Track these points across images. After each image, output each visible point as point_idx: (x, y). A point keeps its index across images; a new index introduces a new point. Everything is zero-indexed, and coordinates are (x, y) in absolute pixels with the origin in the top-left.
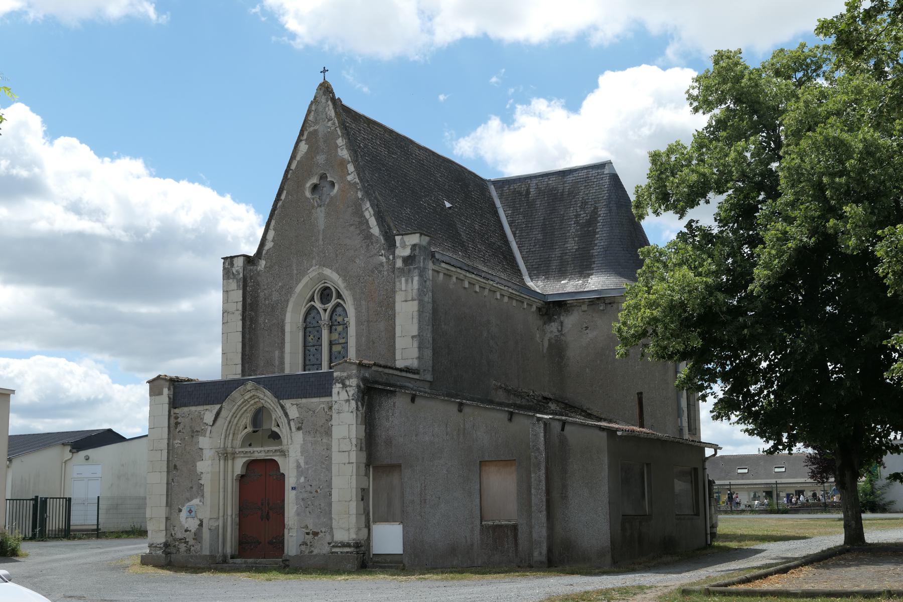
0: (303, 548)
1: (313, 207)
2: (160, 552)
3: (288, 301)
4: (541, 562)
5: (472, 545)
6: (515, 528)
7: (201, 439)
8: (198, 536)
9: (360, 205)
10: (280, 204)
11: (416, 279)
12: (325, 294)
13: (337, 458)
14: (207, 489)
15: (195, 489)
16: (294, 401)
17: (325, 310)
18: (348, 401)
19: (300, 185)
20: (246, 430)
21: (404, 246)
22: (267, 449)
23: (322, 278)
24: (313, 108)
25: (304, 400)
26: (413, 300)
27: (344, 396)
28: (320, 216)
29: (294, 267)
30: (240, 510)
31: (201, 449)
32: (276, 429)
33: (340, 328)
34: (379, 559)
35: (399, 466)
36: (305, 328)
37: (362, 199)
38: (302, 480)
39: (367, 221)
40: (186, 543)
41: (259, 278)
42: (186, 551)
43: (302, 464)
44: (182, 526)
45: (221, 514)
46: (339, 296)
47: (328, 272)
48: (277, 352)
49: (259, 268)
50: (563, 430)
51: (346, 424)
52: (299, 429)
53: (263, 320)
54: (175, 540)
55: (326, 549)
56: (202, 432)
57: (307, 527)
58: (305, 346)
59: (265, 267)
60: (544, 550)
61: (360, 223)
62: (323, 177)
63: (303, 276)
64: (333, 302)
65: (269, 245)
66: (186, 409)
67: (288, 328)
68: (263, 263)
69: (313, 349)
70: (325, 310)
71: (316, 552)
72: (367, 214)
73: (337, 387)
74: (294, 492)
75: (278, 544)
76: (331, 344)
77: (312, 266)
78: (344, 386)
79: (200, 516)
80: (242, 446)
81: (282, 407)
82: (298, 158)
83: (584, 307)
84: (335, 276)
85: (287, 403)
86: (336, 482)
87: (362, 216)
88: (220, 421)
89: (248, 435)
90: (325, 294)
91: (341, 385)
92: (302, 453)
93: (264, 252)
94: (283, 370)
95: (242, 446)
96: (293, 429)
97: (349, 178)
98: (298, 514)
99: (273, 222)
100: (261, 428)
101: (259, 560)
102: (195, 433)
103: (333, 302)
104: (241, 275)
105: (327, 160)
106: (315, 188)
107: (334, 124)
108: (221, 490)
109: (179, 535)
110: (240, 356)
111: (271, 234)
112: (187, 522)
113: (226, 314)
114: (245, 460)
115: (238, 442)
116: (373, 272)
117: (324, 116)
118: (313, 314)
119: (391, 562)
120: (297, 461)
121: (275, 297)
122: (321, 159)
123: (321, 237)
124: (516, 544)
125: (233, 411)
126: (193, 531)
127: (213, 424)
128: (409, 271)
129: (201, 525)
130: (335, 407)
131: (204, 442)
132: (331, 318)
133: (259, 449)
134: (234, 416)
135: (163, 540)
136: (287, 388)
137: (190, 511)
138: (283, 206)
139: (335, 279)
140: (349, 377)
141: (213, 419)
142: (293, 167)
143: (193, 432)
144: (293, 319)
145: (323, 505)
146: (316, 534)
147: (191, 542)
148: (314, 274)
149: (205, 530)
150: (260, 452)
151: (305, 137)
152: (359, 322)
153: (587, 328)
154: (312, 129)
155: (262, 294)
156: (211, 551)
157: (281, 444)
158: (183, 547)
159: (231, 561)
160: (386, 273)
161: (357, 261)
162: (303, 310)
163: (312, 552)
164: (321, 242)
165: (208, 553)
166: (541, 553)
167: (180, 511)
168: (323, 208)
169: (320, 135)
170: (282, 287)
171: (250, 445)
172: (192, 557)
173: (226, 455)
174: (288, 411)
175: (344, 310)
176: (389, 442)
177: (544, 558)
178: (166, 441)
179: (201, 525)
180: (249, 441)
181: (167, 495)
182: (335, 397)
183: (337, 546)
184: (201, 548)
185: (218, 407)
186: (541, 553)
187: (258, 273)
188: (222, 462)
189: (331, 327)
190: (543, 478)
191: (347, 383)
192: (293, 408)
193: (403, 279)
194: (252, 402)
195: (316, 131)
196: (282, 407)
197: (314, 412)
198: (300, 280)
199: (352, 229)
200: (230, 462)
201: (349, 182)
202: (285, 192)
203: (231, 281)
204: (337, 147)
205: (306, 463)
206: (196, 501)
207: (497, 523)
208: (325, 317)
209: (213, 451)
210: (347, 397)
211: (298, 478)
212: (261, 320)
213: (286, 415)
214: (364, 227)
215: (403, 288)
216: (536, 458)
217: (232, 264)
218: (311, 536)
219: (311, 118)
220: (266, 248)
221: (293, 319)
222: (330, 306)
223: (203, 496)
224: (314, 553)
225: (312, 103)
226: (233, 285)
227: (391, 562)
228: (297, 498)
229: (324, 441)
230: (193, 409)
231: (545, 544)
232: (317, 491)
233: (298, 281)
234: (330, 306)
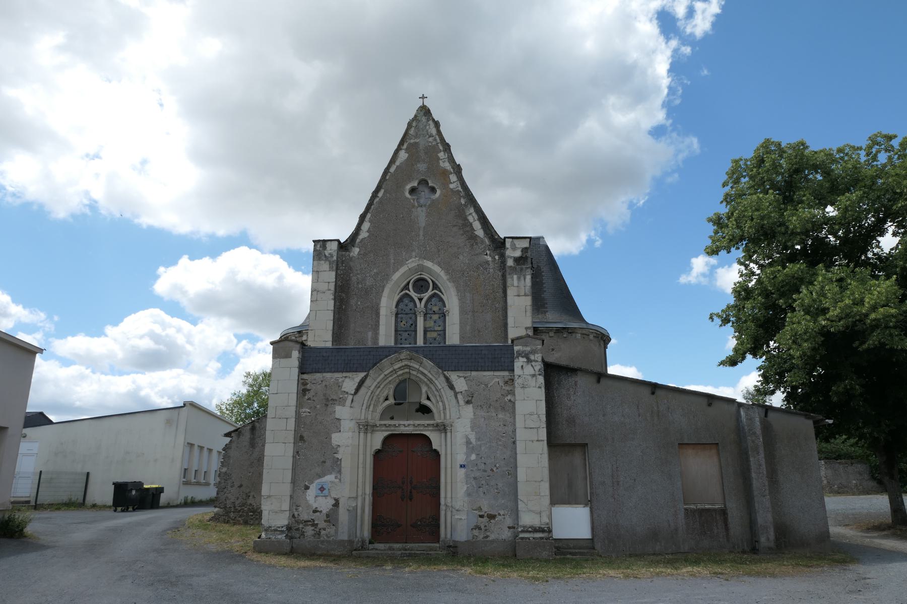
0: (476, 532)
1: (414, 206)
2: (282, 537)
3: (384, 287)
4: (770, 548)
5: (676, 530)
6: (724, 512)
7: (338, 408)
8: (331, 518)
9: (463, 210)
10: (377, 200)
11: (529, 278)
12: (421, 285)
13: (521, 435)
14: (346, 465)
15: (328, 464)
16: (461, 374)
17: (420, 300)
18: (534, 376)
20: (387, 403)
21: (514, 248)
22: (417, 422)
23: (421, 268)
24: (414, 124)
25: (474, 373)
26: (525, 295)
27: (529, 370)
28: (421, 216)
29: (392, 257)
30: (374, 489)
31: (339, 420)
32: (427, 403)
33: (435, 317)
34: (560, 545)
35: (584, 445)
36: (397, 314)
37: (465, 205)
38: (473, 457)
39: (471, 224)
40: (315, 525)
41: (352, 264)
42: (314, 536)
43: (473, 440)
44: (309, 506)
45: (360, 493)
46: (435, 286)
47: (429, 264)
48: (370, 334)
50: (766, 415)
51: (530, 399)
52: (468, 402)
53: (355, 302)
54: (298, 522)
55: (507, 534)
56: (342, 402)
57: (480, 509)
58: (396, 331)
59: (359, 254)
60: (772, 536)
61: (463, 225)
62: (423, 182)
63: (402, 266)
64: (430, 292)
65: (363, 235)
66: (318, 376)
67: (383, 312)
68: (356, 251)
69: (405, 335)
70: (420, 300)
71: (492, 537)
72: (471, 219)
73: (519, 363)
74: (463, 470)
75: (430, 527)
76: (425, 331)
77: (411, 258)
78: (529, 361)
79: (334, 495)
80: (381, 419)
81: (447, 379)
82: (398, 163)
83: (552, 334)
84: (436, 268)
85: (453, 376)
86: (522, 460)
87: (466, 219)
88: (363, 390)
89: (389, 407)
90: (421, 285)
91: (525, 360)
92: (472, 429)
93: (358, 240)
94: (416, 343)
95: (381, 419)
96: (462, 402)
97: (452, 186)
98: (469, 495)
99: (369, 216)
100: (405, 398)
101: (409, 546)
102: (329, 402)
103: (430, 292)
104: (335, 258)
106: (413, 191)
107: (435, 140)
108: (361, 466)
109: (305, 516)
110: (331, 333)
111: (366, 226)
112: (315, 500)
113: (315, 293)
114: (386, 434)
115: (378, 415)
116: (478, 268)
117: (425, 132)
118: (406, 301)
119: (574, 548)
120: (467, 437)
121: (369, 282)
122: (422, 167)
123: (421, 233)
124: (727, 528)
125: (378, 380)
126: (324, 512)
127: (356, 393)
128: (522, 270)
129: (337, 504)
130: (518, 382)
131: (342, 412)
132: (426, 306)
133: (406, 423)
134: (377, 387)
135: (286, 523)
137: (322, 489)
138: (380, 202)
139: (435, 270)
140: (533, 352)
141: (355, 386)
142: (392, 170)
143: (327, 400)
144: (387, 304)
145: (500, 485)
146: (492, 517)
147: (322, 524)
148: (414, 265)
149: (342, 510)
150: (407, 426)
151: (405, 146)
152: (462, 312)
153: (553, 350)
154: (412, 141)
155: (354, 279)
156: (349, 536)
157: (433, 418)
158: (309, 531)
159: (371, 546)
160: (491, 270)
161: (461, 257)
162: (397, 298)
163: (487, 537)
164: (421, 237)
165: (346, 538)
166: (768, 539)
167: (307, 488)
168: (424, 209)
169: (421, 147)
170: (377, 274)
171: (392, 418)
172: (322, 542)
173: (367, 428)
174: (454, 383)
175: (442, 300)
176: (571, 421)
177: (772, 545)
178: (293, 409)
179: (337, 504)
180: (389, 414)
181: (294, 469)
182: (518, 371)
183: (527, 532)
184: (336, 532)
185: (362, 375)
186: (768, 539)
187: (351, 259)
188: (362, 435)
189: (425, 315)
190: (763, 462)
191: (532, 357)
192: (460, 382)
193: (515, 277)
194: (401, 372)
195: (416, 143)
196: (447, 379)
197: (486, 385)
198: (398, 270)
199: (455, 229)
200: (369, 435)
201: (452, 190)
202: (382, 191)
203: (323, 262)
204: (439, 159)
205: (478, 439)
206: (330, 478)
207: (699, 506)
208: (421, 306)
209: (354, 422)
210: (532, 372)
211: (468, 455)
212: (353, 302)
213: (452, 387)
214: (468, 229)
215: (516, 283)
216: (753, 442)
217: (324, 247)
218: (486, 519)
219: (412, 132)
220: (361, 237)
221: (387, 304)
222: (426, 296)
223: (340, 472)
224: (490, 539)
225: (413, 120)
226: (325, 266)
227: (574, 548)
228: (467, 476)
229: (500, 416)
230: (328, 375)
231: (772, 529)
232: (492, 470)
233: (396, 270)
234: (426, 296)
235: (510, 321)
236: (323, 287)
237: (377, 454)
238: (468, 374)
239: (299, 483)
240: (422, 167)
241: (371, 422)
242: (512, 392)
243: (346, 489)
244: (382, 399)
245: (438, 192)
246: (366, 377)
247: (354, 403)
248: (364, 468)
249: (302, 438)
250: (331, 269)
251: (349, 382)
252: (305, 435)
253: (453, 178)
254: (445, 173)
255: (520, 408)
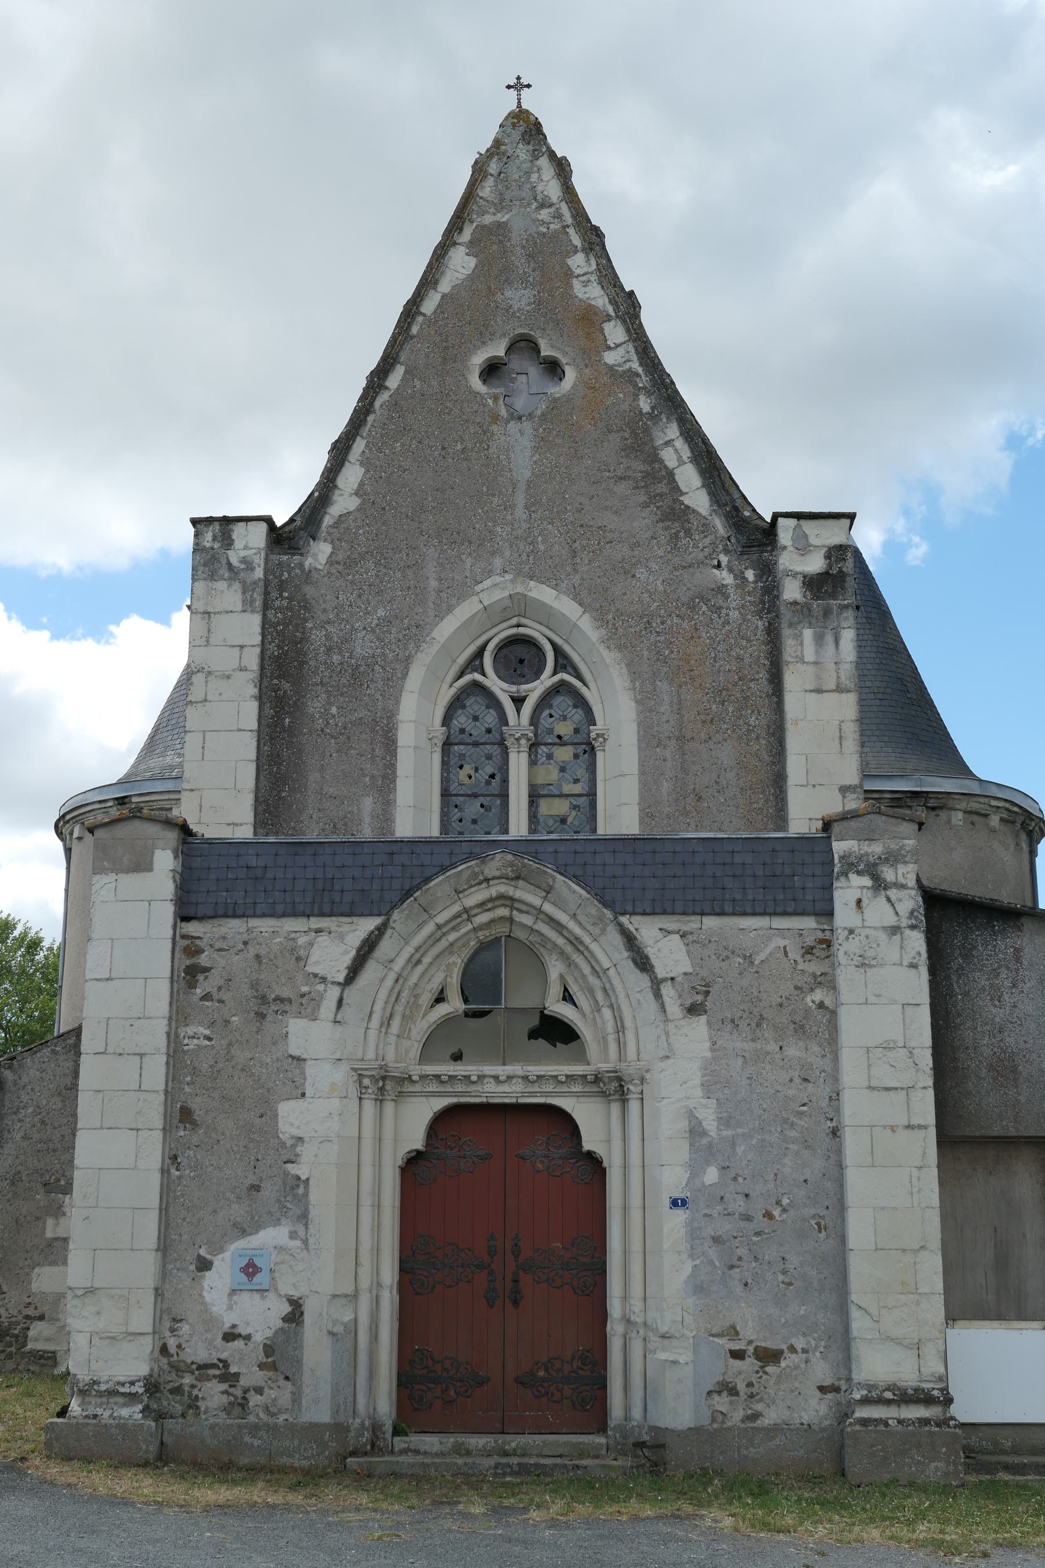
0: (721, 1402)
1: (495, 418)
2: (132, 1413)
3: (408, 661)
7: (296, 1026)
8: (280, 1356)
9: (647, 431)
10: (383, 397)
11: (848, 636)
12: (520, 656)
13: (857, 1109)
14: (322, 1198)
15: (270, 1192)
17: (518, 701)
18: (895, 930)
19: (451, 357)
20: (443, 1009)
21: (804, 548)
22: (535, 1070)
24: (493, 167)
25: (711, 922)
26: (839, 689)
27: (879, 913)
28: (519, 448)
29: (431, 570)
31: (298, 1059)
33: (564, 754)
34: (973, 1441)
36: (447, 744)
37: (651, 416)
38: (712, 1175)
39: (671, 475)
40: (229, 1378)
42: (227, 1409)
43: (711, 1126)
44: (210, 1320)
45: (365, 1281)
46: (563, 661)
47: (543, 593)
48: (368, 804)
49: (309, 562)
52: (693, 1010)
54: (178, 1369)
55: (815, 1410)
56: (306, 1005)
57: (733, 1332)
58: (445, 794)
59: (331, 561)
61: (647, 475)
62: (523, 345)
63: (461, 598)
64: (547, 680)
67: (406, 736)
69: (473, 808)
70: (518, 701)
71: (771, 1416)
72: (669, 457)
73: (848, 891)
74: (680, 1216)
75: (577, 1383)
76: (535, 796)
77: (490, 574)
78: (879, 885)
79: (287, 1287)
81: (630, 940)
82: (445, 286)
84: (567, 607)
85: (648, 931)
86: (859, 1184)
87: (654, 458)
89: (448, 1021)
90: (520, 656)
91: (867, 881)
93: (327, 521)
95: (426, 1054)
96: (674, 1009)
97: (611, 358)
98: (699, 1289)
99: (359, 446)
101: (515, 1441)
102: (267, 1006)
103: (547, 680)
104: (259, 573)
105: (539, 303)
106: (492, 370)
107: (558, 216)
108: (366, 1201)
109: (198, 1352)
110: (249, 800)
111: (351, 476)
112: (231, 1304)
114: (440, 1103)
116: (693, 608)
117: (526, 193)
119: (1015, 1450)
120: (691, 1115)
121: (363, 646)
122: (519, 298)
123: (520, 499)
126: (259, 1338)
128: (827, 612)
129: (295, 1315)
130: (845, 949)
131: (308, 1036)
132: (534, 720)
134: (414, 962)
136: (648, 878)
137: (251, 1269)
138: (394, 404)
139: (563, 611)
140: (893, 858)
141: (347, 960)
142: (429, 306)
143: (263, 999)
145: (794, 1261)
146: (768, 1356)
147: (251, 1376)
148: (498, 595)
150: (506, 1079)
151: (466, 235)
152: (649, 738)
154: (488, 219)
155: (317, 636)
156: (336, 1412)
157: (582, 1057)
158: (213, 1395)
159: (399, 1443)
160: (734, 615)
161: (641, 573)
162: (447, 695)
163: (756, 1416)
164: (520, 513)
165: (325, 1418)
167: (204, 1265)
168: (527, 426)
169: (516, 237)
171: (457, 1057)
173: (383, 1085)
174: (651, 952)
176: (1006, 1069)
178: (161, 1027)
179: (295, 1315)
182: (844, 915)
183: (881, 1401)
184: (296, 1398)
185: (368, 925)
187: (307, 576)
188: (369, 1106)
189: (533, 746)
191: (888, 874)
192: (668, 946)
193: (808, 634)
194: (483, 918)
195: (500, 225)
196: (630, 940)
197: (749, 959)
198: (450, 610)
199: (621, 488)
200: (389, 1107)
201: (611, 368)
203: (222, 585)
204: (569, 274)
205: (725, 1121)
206: (273, 1237)
208: (519, 721)
209: (344, 1067)
210: (891, 920)
211: (695, 1170)
212: (314, 706)
213: (643, 964)
214: (662, 488)
217: (227, 541)
218: (750, 1364)
219: (487, 190)
221: (418, 713)
223: (304, 1217)
224: (765, 1422)
226: (230, 596)
227: (1015, 1450)
228: (693, 1233)
230: (264, 925)
232: (768, 1215)
233: (444, 611)
235: (795, 768)
236: (224, 659)
237: (413, 1163)
238: (692, 923)
239: (181, 1253)
240: (519, 298)
241: (397, 1068)
242: (827, 981)
243: (324, 1273)
244: (426, 998)
245: (570, 375)
246: (381, 930)
247: (346, 1013)
248: (377, 1206)
249: (186, 1115)
250: (248, 606)
251: (331, 946)
252: (196, 1105)
253: (615, 332)
254: (589, 320)
255: (857, 1027)
